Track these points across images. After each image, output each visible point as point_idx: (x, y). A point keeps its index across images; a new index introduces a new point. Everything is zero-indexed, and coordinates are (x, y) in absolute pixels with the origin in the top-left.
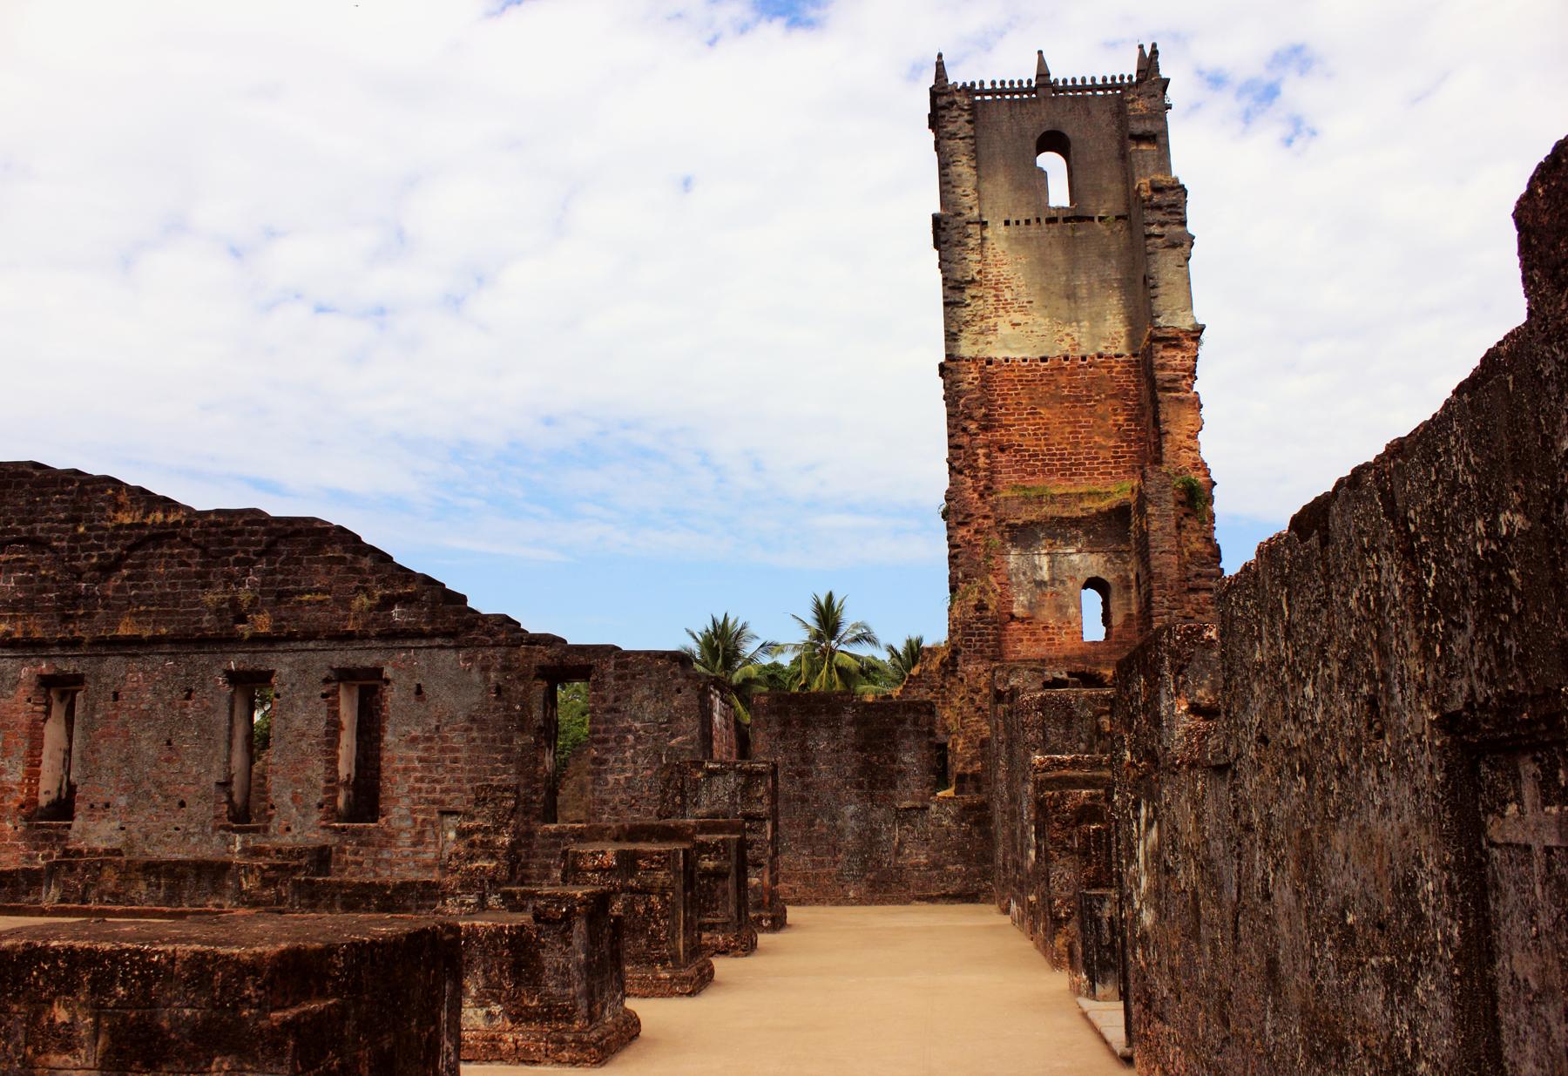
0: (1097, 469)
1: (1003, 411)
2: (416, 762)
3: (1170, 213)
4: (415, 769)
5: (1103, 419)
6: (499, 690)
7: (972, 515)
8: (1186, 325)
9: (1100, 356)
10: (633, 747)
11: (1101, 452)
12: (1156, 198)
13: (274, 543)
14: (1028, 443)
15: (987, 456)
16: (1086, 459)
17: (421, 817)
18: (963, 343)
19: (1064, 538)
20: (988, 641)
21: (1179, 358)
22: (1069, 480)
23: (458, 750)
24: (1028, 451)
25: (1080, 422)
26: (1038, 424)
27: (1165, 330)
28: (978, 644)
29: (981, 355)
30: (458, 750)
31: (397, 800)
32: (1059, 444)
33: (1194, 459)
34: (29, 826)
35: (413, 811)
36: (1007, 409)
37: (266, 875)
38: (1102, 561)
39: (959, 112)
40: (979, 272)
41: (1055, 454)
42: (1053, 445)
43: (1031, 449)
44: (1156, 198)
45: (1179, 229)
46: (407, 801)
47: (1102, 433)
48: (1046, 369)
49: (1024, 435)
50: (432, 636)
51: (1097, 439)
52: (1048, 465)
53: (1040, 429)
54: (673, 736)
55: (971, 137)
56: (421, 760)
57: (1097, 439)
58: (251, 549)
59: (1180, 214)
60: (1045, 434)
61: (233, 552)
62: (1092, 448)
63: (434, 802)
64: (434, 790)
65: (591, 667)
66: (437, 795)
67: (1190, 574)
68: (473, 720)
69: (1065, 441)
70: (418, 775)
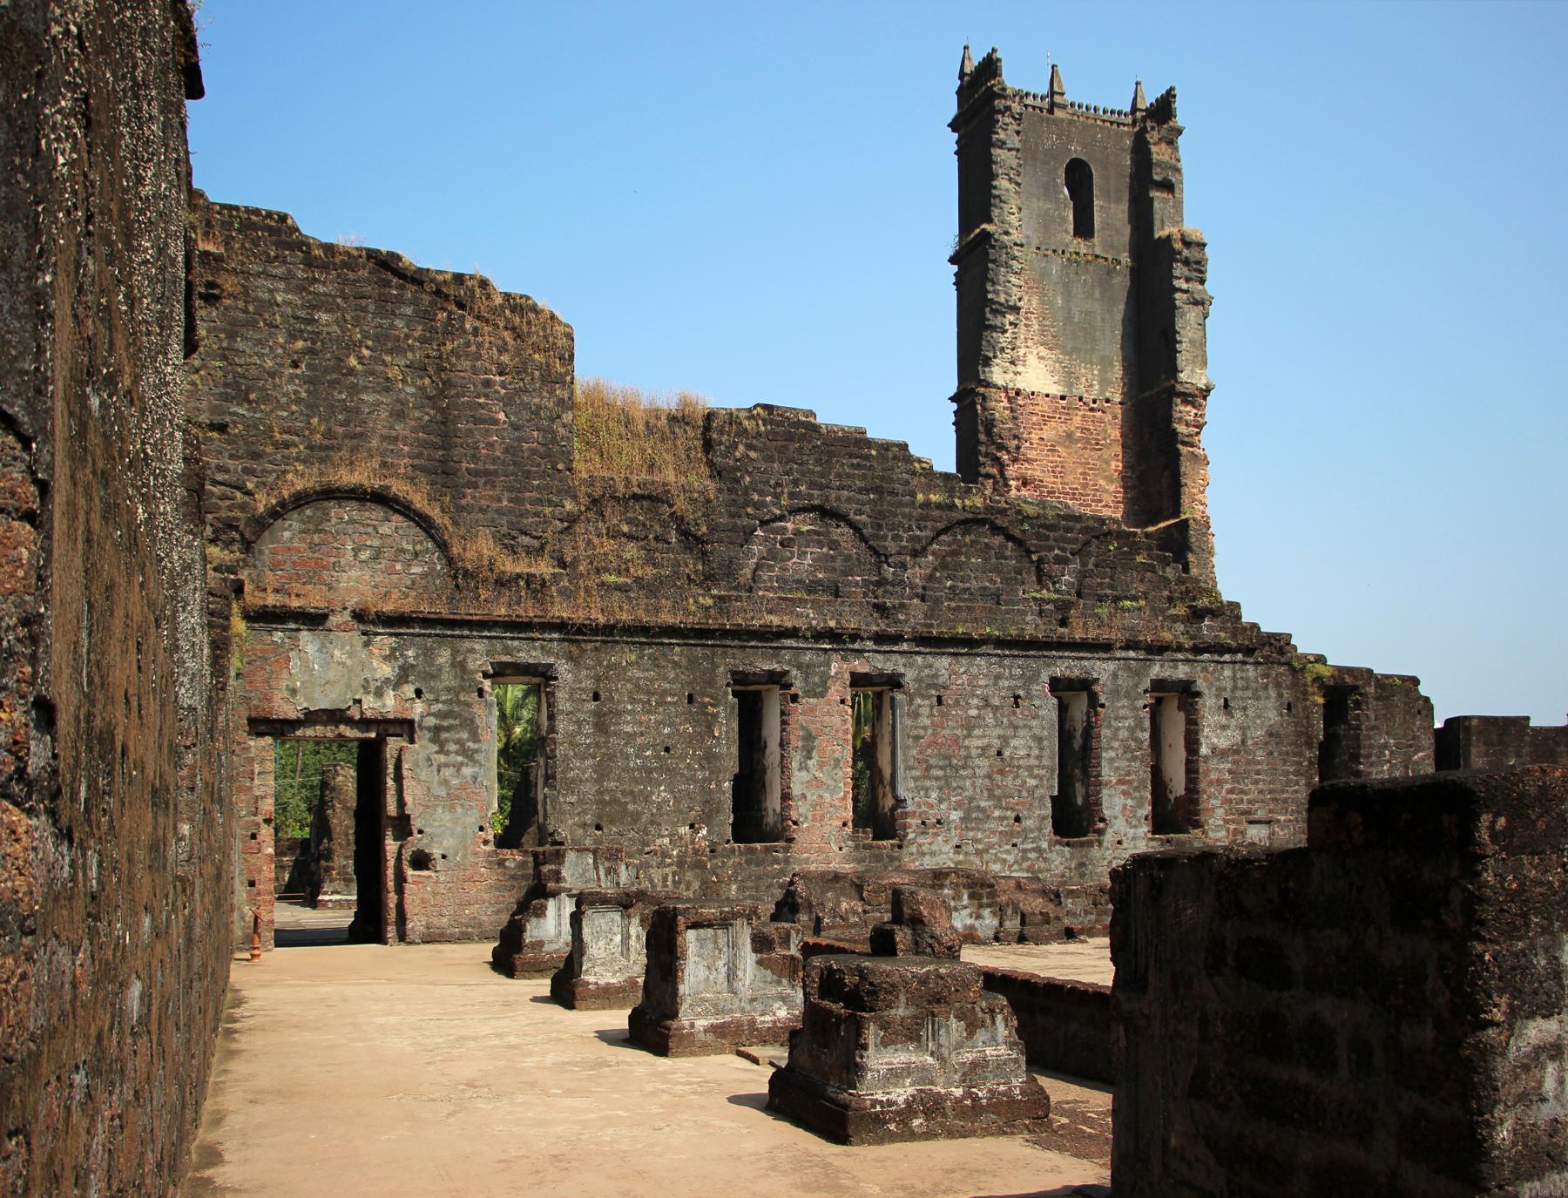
4: (1226, 781)
6: (1289, 707)
10: (1389, 761)
13: (1087, 543)
17: (1232, 827)
23: (1259, 763)
30: (1259, 763)
34: (857, 847)
35: (1227, 822)
46: (1220, 812)
58: (1069, 546)
61: (1051, 549)
64: (1242, 801)
66: (1244, 806)
68: (1271, 735)
70: (1229, 786)
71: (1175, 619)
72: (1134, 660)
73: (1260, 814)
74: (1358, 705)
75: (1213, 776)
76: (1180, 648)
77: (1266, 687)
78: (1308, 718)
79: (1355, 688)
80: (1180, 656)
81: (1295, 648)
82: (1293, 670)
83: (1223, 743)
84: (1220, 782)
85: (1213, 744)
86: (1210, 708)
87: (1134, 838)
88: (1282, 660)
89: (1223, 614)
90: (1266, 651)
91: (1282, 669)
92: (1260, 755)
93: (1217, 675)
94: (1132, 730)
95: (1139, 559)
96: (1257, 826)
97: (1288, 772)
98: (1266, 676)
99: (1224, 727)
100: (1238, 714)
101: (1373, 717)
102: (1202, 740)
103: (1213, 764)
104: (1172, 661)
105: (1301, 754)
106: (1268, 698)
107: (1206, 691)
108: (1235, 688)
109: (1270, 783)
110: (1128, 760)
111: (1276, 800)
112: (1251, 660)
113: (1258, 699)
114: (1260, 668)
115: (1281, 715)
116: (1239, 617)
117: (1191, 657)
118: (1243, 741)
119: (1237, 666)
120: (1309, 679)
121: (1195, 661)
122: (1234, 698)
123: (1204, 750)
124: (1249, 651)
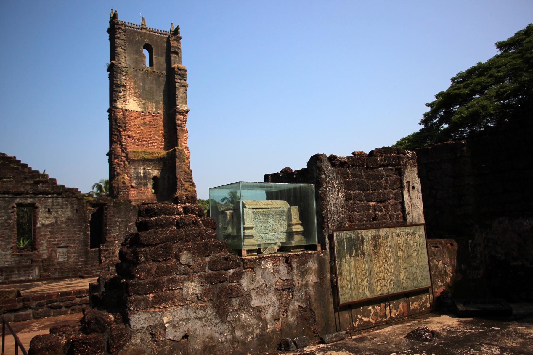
0: (156, 146)
1: (130, 126)
2: (49, 232)
3: (183, 77)
4: (48, 235)
6: (77, 210)
7: (120, 156)
8: (185, 109)
9: (158, 113)
11: (157, 141)
12: (179, 72)
14: (138, 137)
15: (125, 139)
16: (153, 142)
18: (118, 103)
19: (147, 165)
20: (126, 193)
21: (182, 118)
22: (148, 148)
23: (63, 228)
24: (136, 138)
28: (123, 194)
29: (124, 108)
31: (41, 245)
32: (146, 137)
33: (186, 146)
36: (131, 125)
37: (45, 268)
38: (157, 172)
39: (122, 31)
40: (125, 83)
41: (144, 140)
42: (144, 137)
44: (179, 72)
45: (185, 82)
48: (143, 115)
49: (136, 134)
50: (53, 194)
51: (156, 137)
52: (142, 143)
54: (130, 223)
55: (125, 40)
56: (50, 232)
57: (156, 137)
59: (185, 78)
60: (142, 134)
62: (155, 139)
63: (55, 244)
64: (55, 241)
65: (106, 204)
67: (185, 177)
70: (49, 236)
71: (27, 184)
72: (7, 197)
73: (63, 245)
74: (106, 208)
75: (42, 233)
76: (28, 193)
77: (67, 204)
78: (84, 214)
79: (105, 204)
80: (29, 196)
81: (80, 192)
82: (79, 199)
83: (47, 222)
84: (45, 235)
85: (43, 223)
86: (42, 212)
87: (5, 255)
88: (74, 196)
89: (47, 182)
90: (68, 193)
91: (74, 199)
92: (63, 226)
93: (45, 201)
94: (5, 220)
95: (12, 165)
96: (62, 248)
97: (76, 231)
98: (67, 201)
99: (47, 218)
100: (54, 214)
101: (112, 213)
102: (38, 222)
103: (42, 229)
104: (25, 197)
105: (81, 225)
106: (68, 208)
107: (40, 207)
108: (53, 205)
109: (67, 234)
110: (3, 230)
111: (70, 240)
112: (60, 196)
113: (63, 208)
114: (64, 199)
115: (73, 213)
116: (55, 183)
117: (34, 196)
118: (56, 222)
119: (54, 199)
120: (84, 202)
121: (36, 197)
122: (53, 208)
123: (38, 225)
124: (59, 194)
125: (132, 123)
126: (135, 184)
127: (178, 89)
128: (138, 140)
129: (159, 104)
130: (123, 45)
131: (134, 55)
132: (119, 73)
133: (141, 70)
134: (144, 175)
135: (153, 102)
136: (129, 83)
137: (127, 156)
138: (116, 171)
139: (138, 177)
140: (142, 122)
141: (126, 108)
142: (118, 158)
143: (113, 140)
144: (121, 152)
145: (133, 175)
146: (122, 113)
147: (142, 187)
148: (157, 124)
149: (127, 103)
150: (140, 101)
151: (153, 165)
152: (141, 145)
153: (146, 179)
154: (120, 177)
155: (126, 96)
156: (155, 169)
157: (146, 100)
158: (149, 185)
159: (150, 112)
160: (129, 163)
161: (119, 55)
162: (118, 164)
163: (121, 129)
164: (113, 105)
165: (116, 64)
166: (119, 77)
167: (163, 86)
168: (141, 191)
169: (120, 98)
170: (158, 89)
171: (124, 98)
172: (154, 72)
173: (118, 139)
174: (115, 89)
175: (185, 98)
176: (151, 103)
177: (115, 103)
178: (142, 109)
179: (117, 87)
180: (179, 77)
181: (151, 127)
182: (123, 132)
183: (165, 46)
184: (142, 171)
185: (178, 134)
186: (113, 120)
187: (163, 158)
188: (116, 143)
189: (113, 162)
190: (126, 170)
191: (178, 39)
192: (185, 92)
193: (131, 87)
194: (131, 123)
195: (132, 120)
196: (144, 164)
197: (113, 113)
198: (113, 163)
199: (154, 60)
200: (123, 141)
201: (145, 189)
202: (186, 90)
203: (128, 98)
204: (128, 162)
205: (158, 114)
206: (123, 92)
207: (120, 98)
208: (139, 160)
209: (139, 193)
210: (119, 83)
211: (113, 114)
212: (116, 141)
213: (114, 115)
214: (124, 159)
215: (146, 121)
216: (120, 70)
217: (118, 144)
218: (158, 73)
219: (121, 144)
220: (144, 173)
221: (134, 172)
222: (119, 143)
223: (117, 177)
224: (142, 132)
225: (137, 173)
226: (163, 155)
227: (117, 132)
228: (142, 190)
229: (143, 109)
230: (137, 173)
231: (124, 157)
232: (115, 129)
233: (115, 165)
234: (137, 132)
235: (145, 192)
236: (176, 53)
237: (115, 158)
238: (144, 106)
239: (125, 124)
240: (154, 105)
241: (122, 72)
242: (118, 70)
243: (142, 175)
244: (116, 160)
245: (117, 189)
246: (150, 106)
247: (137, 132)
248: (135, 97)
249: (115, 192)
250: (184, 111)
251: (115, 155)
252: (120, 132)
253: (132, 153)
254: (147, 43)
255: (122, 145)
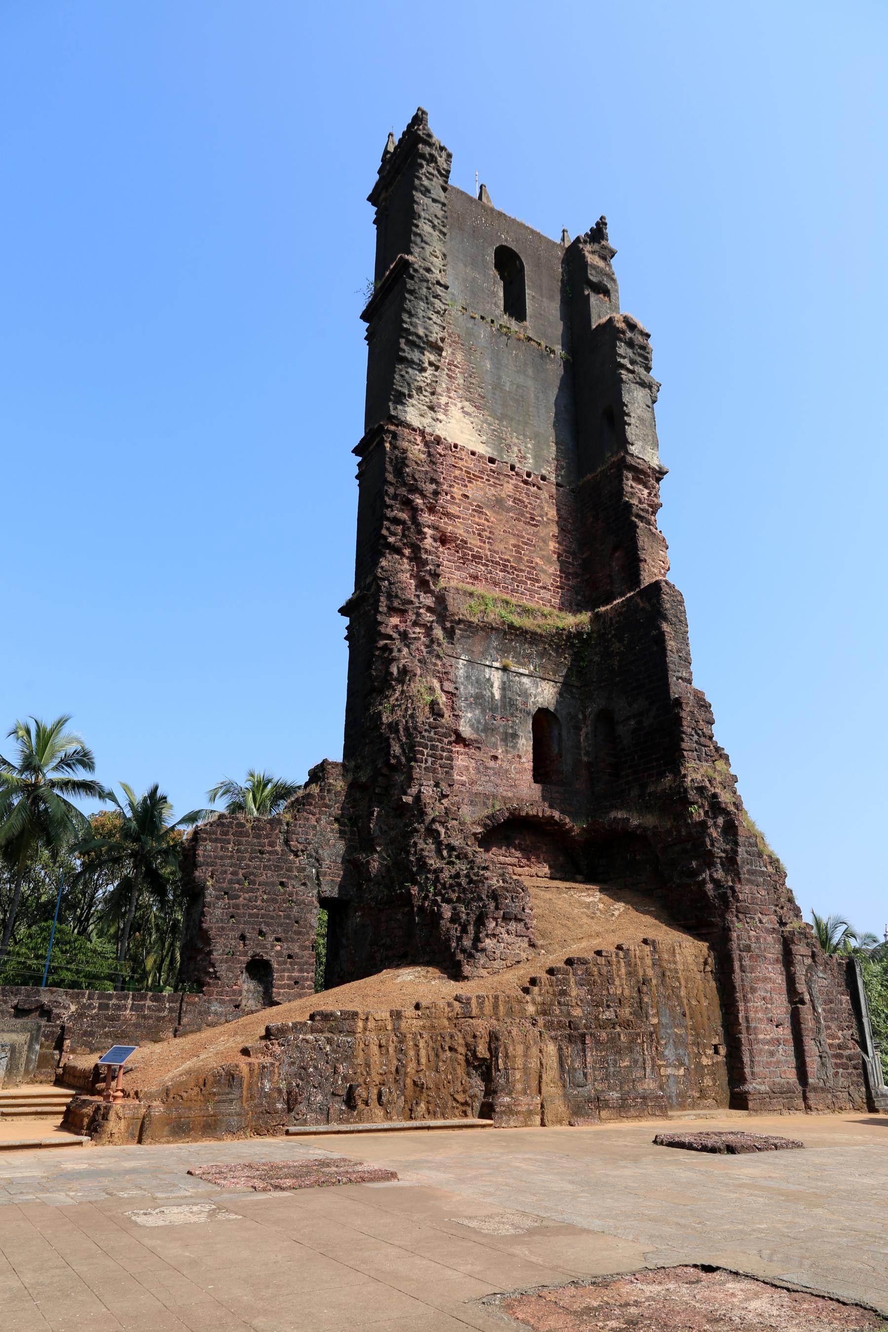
5: (544, 541)
7: (411, 602)
8: (655, 463)
9: (544, 478)
12: (629, 334)
18: (409, 409)
25: (523, 537)
26: (483, 525)
27: (638, 461)
28: (430, 760)
40: (442, 340)
41: (498, 563)
43: (476, 549)
47: (543, 556)
51: (538, 560)
53: (484, 530)
57: (538, 560)
62: (534, 568)
69: (508, 553)
125: (457, 491)
126: (472, 726)
127: (629, 392)
128: (477, 558)
129: (544, 447)
130: (439, 216)
131: (466, 266)
132: (422, 299)
133: (489, 320)
134: (503, 696)
135: (525, 435)
136: (450, 350)
137: (441, 608)
138: (394, 660)
139: (479, 700)
140: (489, 495)
141: (438, 432)
142: (402, 612)
143: (385, 538)
144: (416, 591)
145: (462, 688)
146: (421, 446)
147: (495, 746)
148: (541, 516)
149: (441, 416)
150: (485, 421)
151: (537, 661)
152: (487, 579)
153: (512, 715)
154: (416, 686)
155: (439, 390)
156: (544, 679)
157: (505, 423)
158: (524, 741)
159: (518, 465)
160: (450, 634)
161: (423, 245)
162: (404, 636)
163: (419, 501)
164: (393, 413)
165: (416, 266)
166: (421, 314)
167: (556, 391)
168: (492, 764)
169: (420, 389)
170: (541, 396)
171: (433, 394)
172: (529, 339)
173: (404, 535)
174: (404, 351)
175: (651, 425)
176: (521, 437)
177: (399, 407)
178: (489, 449)
179: (412, 344)
180: (630, 352)
181: (519, 520)
182: (426, 515)
183: (560, 270)
184: (497, 678)
185: (640, 543)
186: (389, 468)
187: (579, 634)
188: (398, 551)
189: (381, 623)
190: (439, 663)
191: (608, 254)
192: (650, 404)
193: (458, 367)
194: (455, 490)
195: (455, 477)
196: (504, 651)
197: (390, 443)
198: (383, 630)
199: (527, 301)
200: (427, 547)
201: (510, 756)
202: (654, 402)
203: (443, 400)
204: (444, 629)
205: (542, 482)
206: (430, 371)
207: (420, 389)
208: (488, 629)
209: (487, 768)
210: (421, 332)
211: (387, 445)
212: (399, 544)
213: (394, 447)
214: (429, 617)
215: (503, 495)
216: (428, 288)
217: (402, 555)
218: (539, 344)
219: (417, 559)
220: (504, 688)
221: (468, 677)
222: (407, 552)
223: (399, 688)
224: (490, 532)
225: (478, 681)
226: (577, 625)
227: (402, 510)
228: (495, 758)
229: (493, 449)
230: (478, 681)
231: (429, 609)
232: (395, 497)
233: (390, 637)
234: (472, 527)
235: (507, 771)
236: (606, 292)
237: (392, 610)
238: (499, 440)
239: (437, 483)
240: (529, 445)
241: (432, 299)
242: (419, 288)
243: (497, 696)
244: (395, 620)
245: (409, 735)
246: (515, 445)
247: (472, 527)
248: (467, 404)
249: (396, 749)
250: (649, 468)
251: (390, 596)
252: (414, 511)
253: (460, 598)
254: (504, 244)
255: (424, 563)
